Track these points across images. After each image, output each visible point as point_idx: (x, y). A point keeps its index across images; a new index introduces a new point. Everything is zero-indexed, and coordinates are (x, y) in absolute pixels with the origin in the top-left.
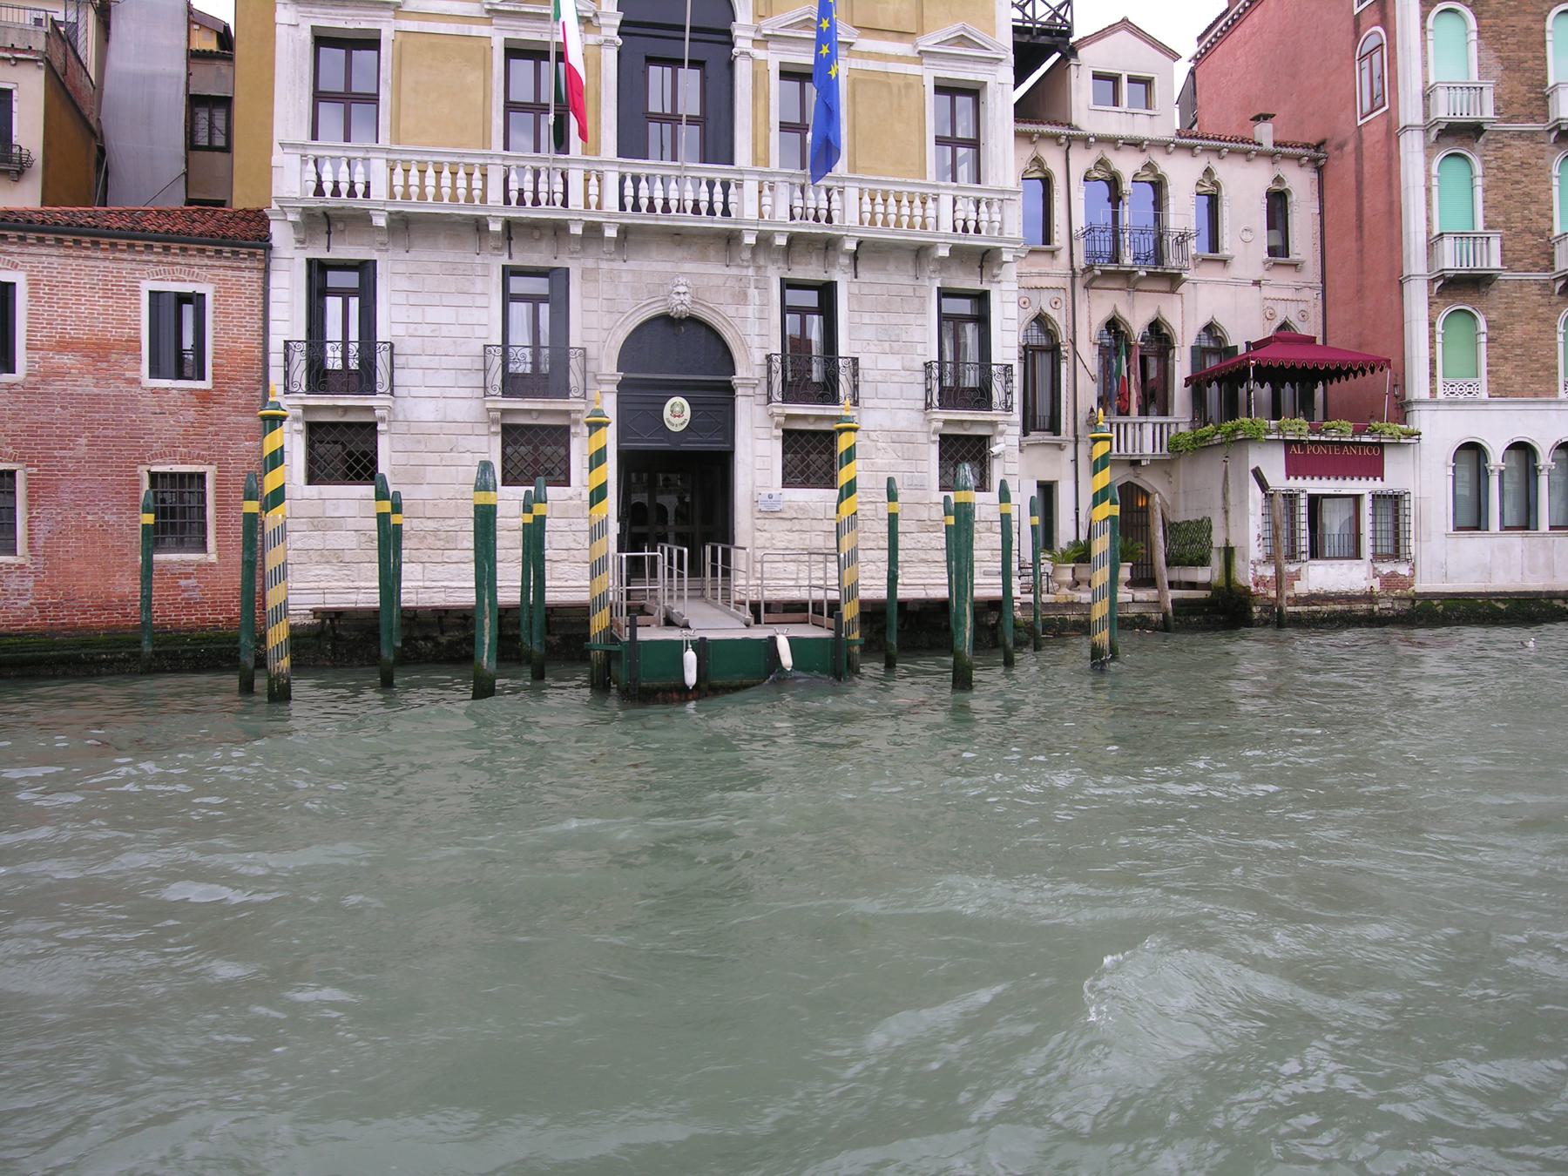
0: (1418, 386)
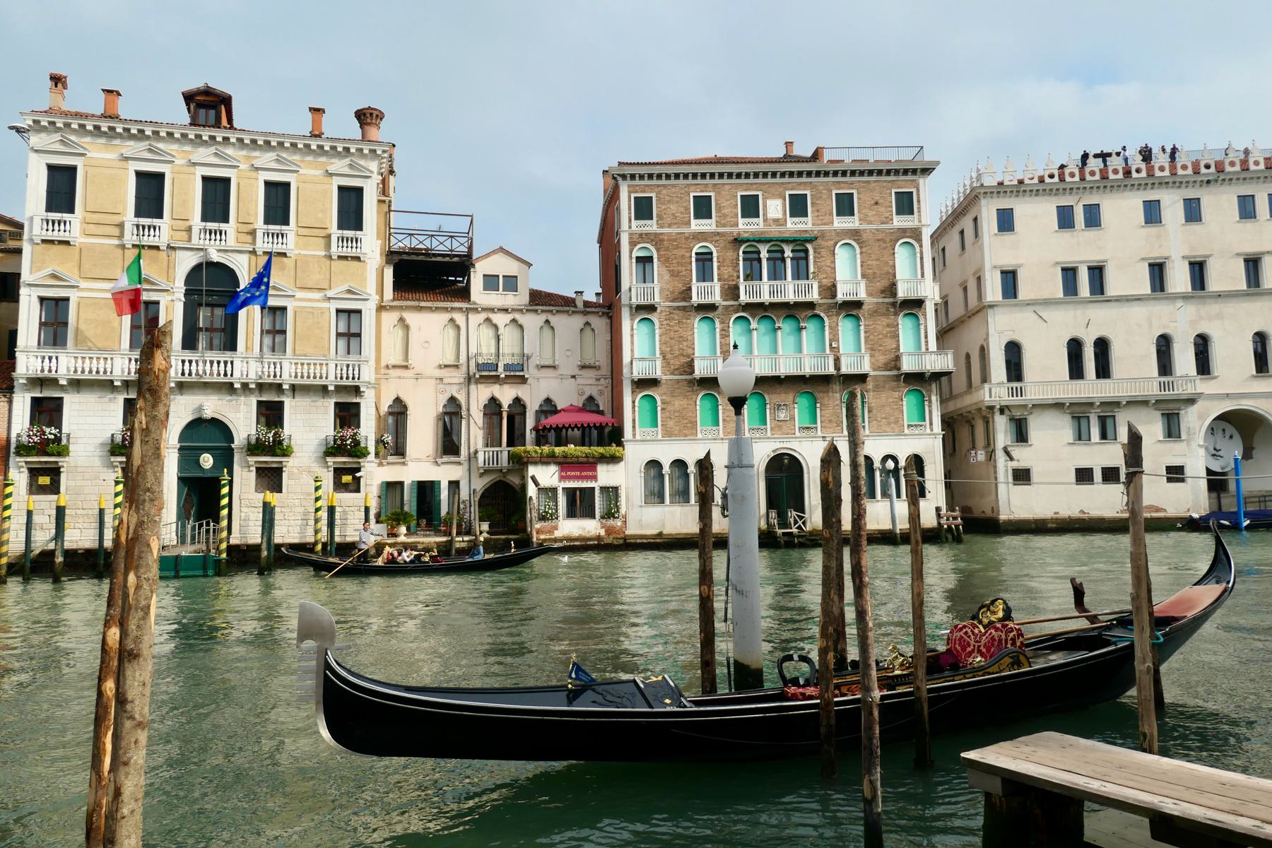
0: (628, 433)
